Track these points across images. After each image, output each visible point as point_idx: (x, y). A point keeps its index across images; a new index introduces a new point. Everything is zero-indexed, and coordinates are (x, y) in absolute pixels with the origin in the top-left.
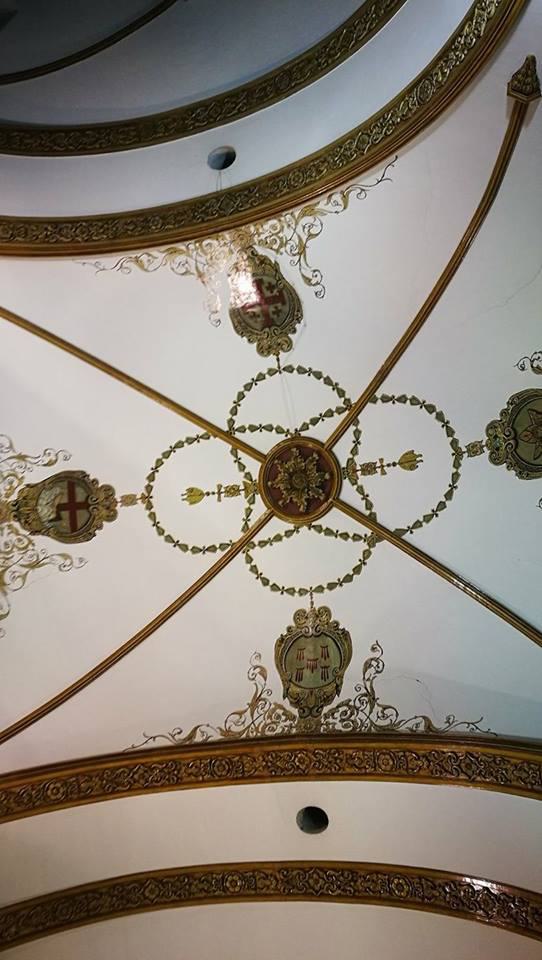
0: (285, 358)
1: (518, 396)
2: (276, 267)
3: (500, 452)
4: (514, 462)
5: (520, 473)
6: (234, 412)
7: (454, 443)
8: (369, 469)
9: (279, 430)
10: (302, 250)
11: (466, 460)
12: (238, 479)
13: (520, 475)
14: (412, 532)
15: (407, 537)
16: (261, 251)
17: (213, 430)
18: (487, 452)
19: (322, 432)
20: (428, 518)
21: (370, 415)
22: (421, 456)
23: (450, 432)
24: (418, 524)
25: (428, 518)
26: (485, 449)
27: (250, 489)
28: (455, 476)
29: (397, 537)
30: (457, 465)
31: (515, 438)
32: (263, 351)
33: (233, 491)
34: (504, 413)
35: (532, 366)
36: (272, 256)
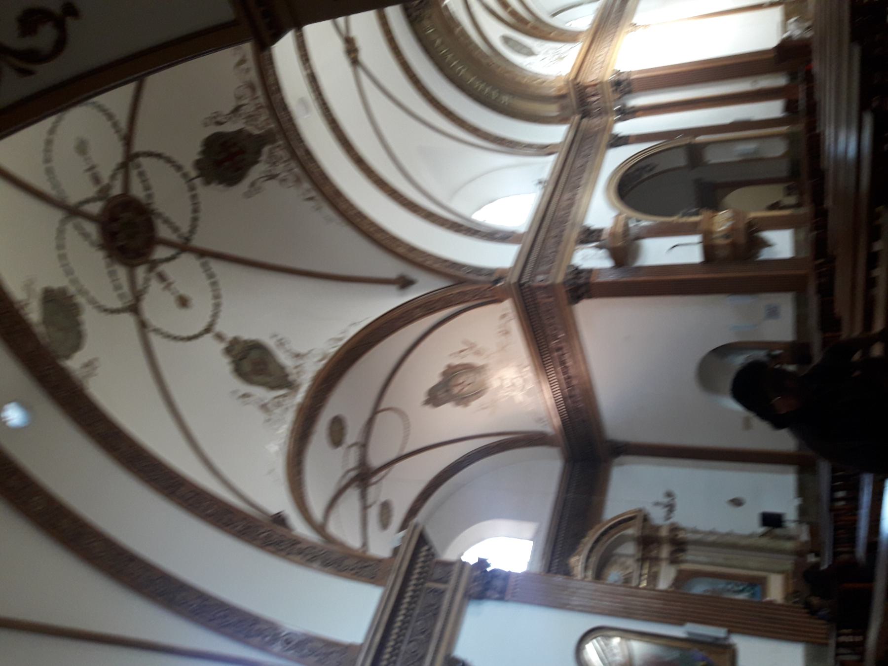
0: (198, 182)
2: (256, 162)
6: (150, 154)
8: (162, 277)
9: (150, 196)
10: (272, 177)
11: (208, 337)
12: (105, 180)
16: (266, 149)
17: (128, 140)
19: (163, 231)
21: (188, 261)
27: (103, 194)
28: (195, 337)
29: (143, 325)
32: (198, 164)
33: (96, 179)
36: (264, 157)
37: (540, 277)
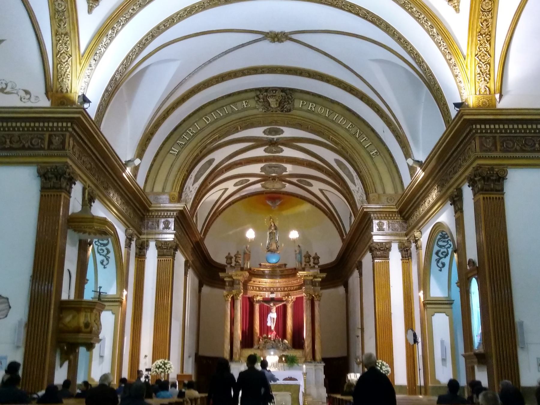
37: (71, 142)
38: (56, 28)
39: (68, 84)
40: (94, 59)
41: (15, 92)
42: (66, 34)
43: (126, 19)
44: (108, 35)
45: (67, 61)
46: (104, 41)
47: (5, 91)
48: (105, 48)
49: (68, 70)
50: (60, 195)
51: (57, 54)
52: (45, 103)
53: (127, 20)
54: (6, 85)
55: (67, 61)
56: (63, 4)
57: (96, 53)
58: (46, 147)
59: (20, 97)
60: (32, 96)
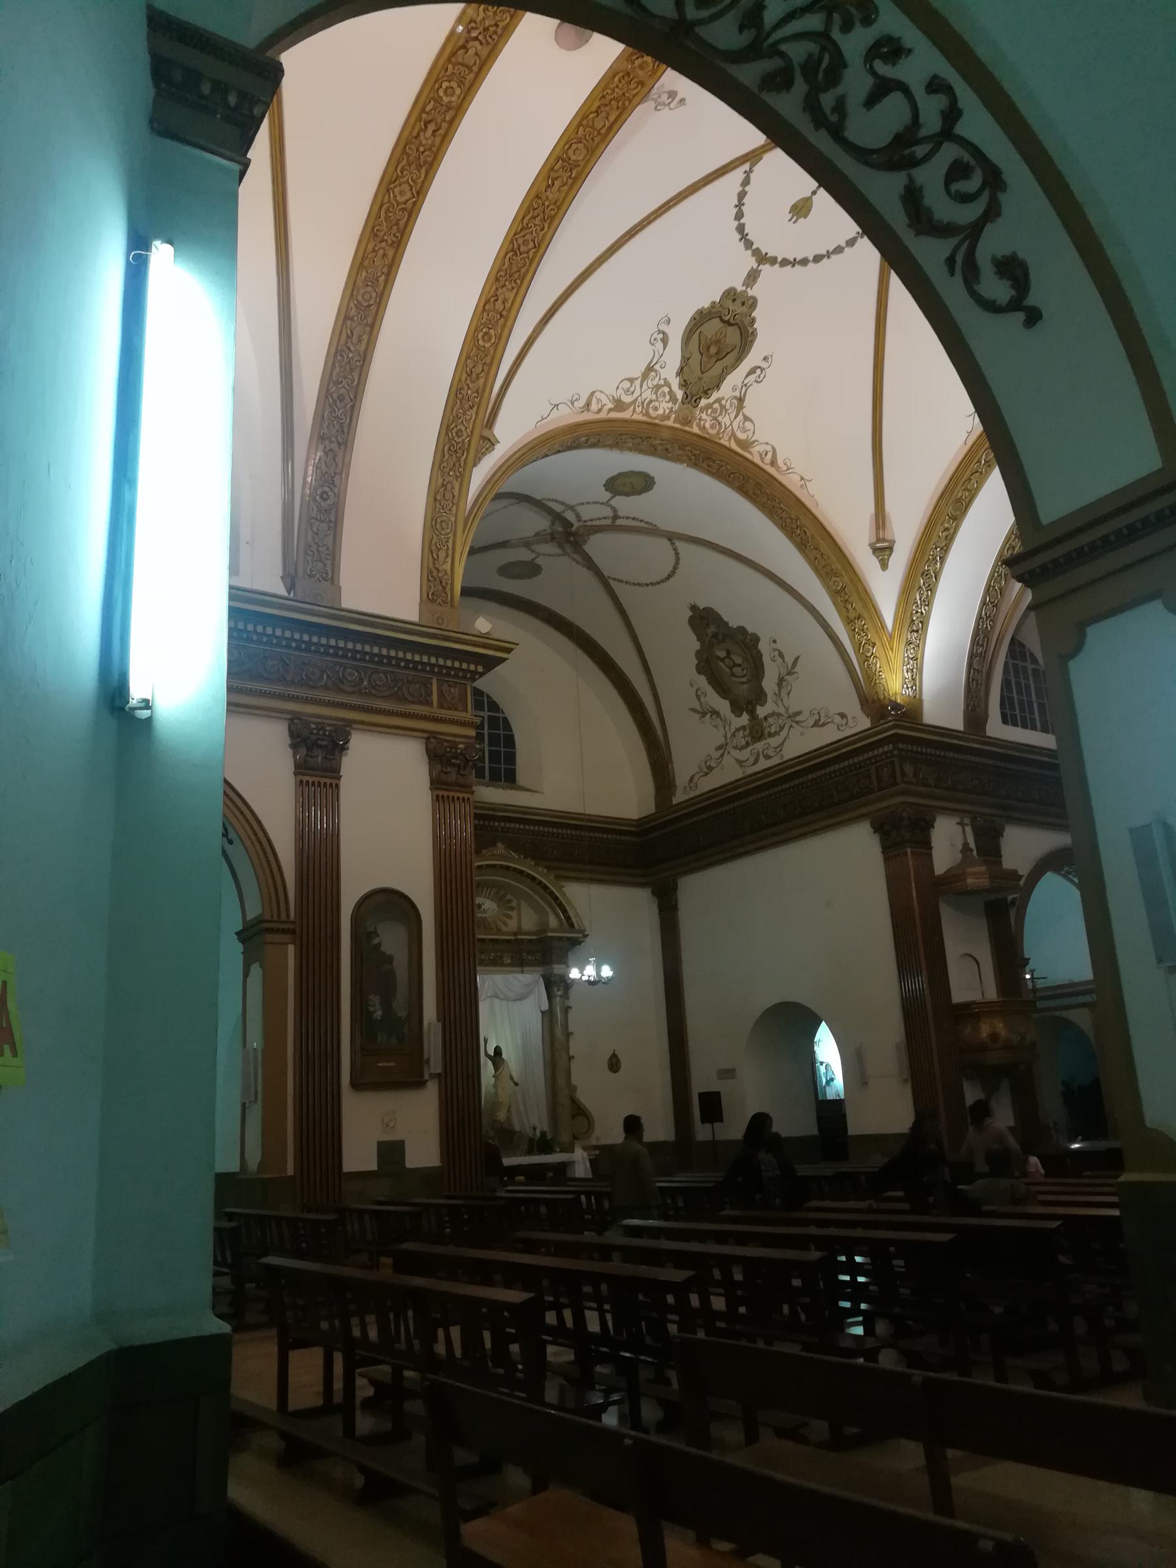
1: (752, 342)
3: (730, 301)
4: (714, 310)
5: (702, 312)
7: (773, 261)
11: (752, 262)
13: (700, 312)
14: (745, 172)
15: (746, 167)
18: (740, 288)
20: (742, 195)
22: (795, 222)
23: (785, 262)
24: (746, 182)
25: (742, 195)
26: (744, 288)
28: (748, 244)
30: (757, 253)
31: (728, 323)
34: (753, 321)
35: (759, 367)
37: (908, 768)
38: (845, 614)
39: (883, 685)
40: (913, 631)
41: (830, 720)
42: (859, 617)
43: (942, 549)
44: (920, 587)
45: (873, 654)
46: (918, 598)
47: (820, 723)
48: (925, 605)
49: (878, 665)
50: (906, 853)
51: (858, 646)
52: (864, 723)
53: (946, 549)
54: (819, 713)
55: (873, 654)
56: (838, 580)
57: (913, 621)
58: (876, 789)
59: (836, 726)
60: (849, 719)
